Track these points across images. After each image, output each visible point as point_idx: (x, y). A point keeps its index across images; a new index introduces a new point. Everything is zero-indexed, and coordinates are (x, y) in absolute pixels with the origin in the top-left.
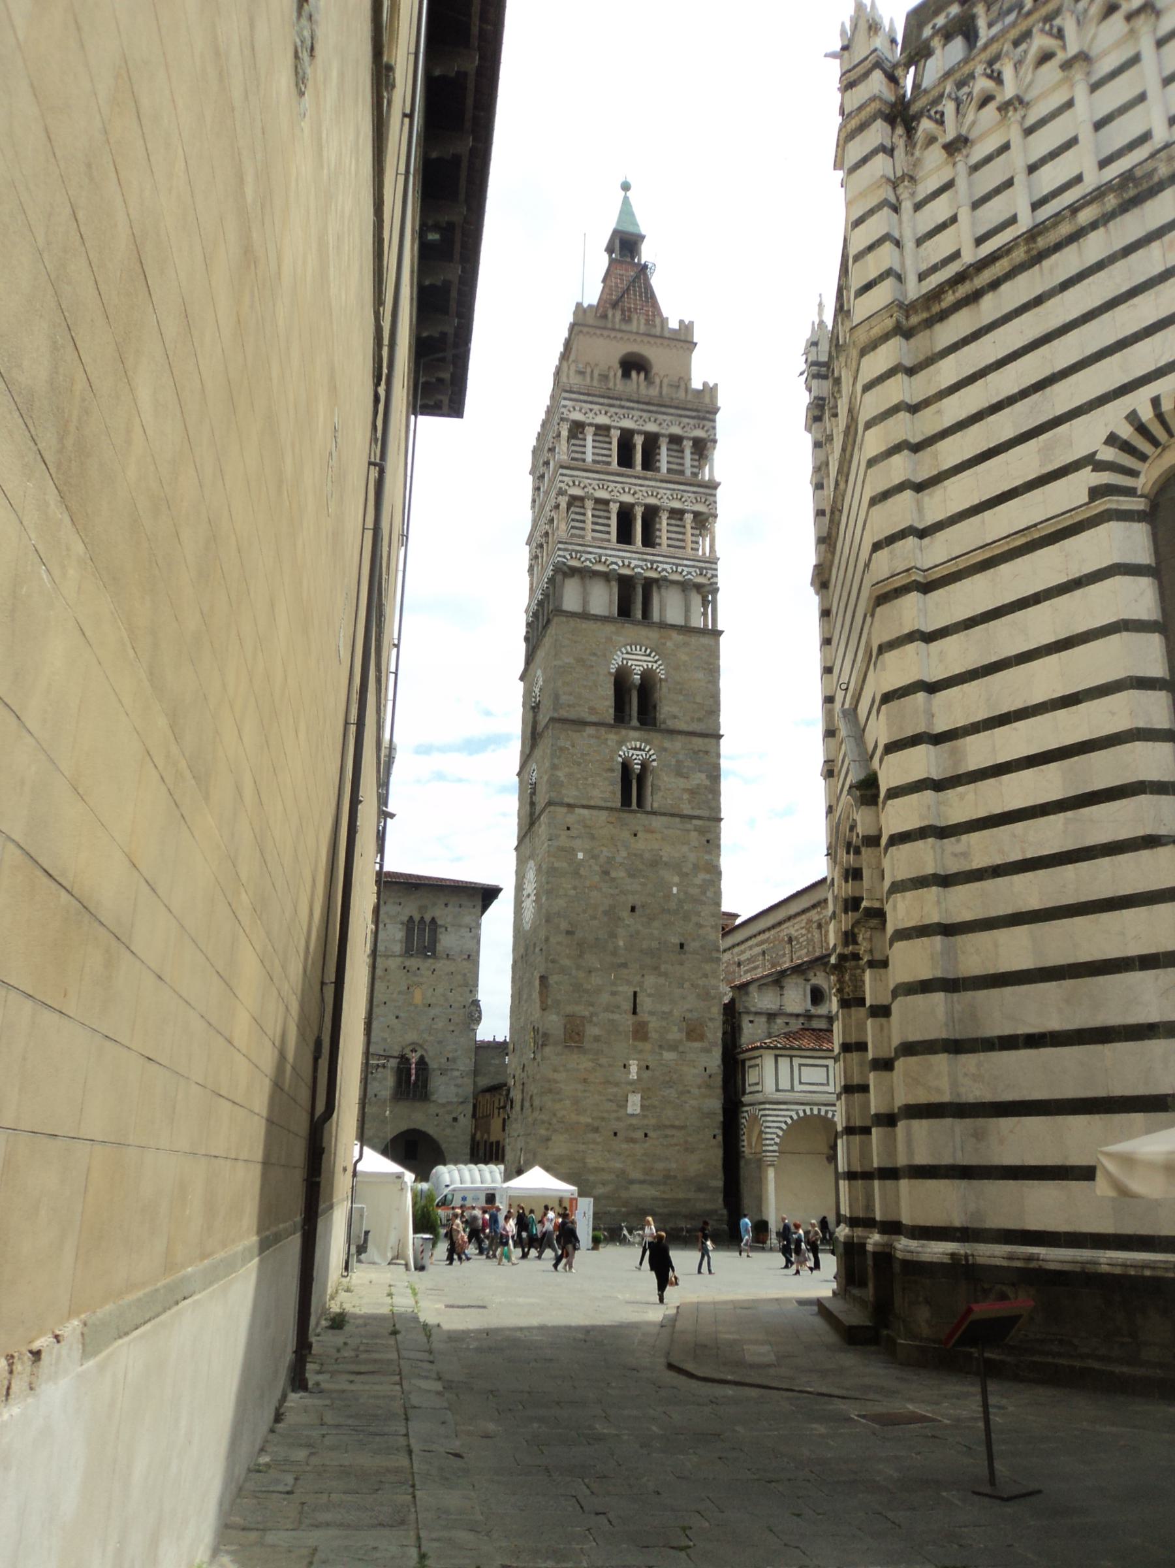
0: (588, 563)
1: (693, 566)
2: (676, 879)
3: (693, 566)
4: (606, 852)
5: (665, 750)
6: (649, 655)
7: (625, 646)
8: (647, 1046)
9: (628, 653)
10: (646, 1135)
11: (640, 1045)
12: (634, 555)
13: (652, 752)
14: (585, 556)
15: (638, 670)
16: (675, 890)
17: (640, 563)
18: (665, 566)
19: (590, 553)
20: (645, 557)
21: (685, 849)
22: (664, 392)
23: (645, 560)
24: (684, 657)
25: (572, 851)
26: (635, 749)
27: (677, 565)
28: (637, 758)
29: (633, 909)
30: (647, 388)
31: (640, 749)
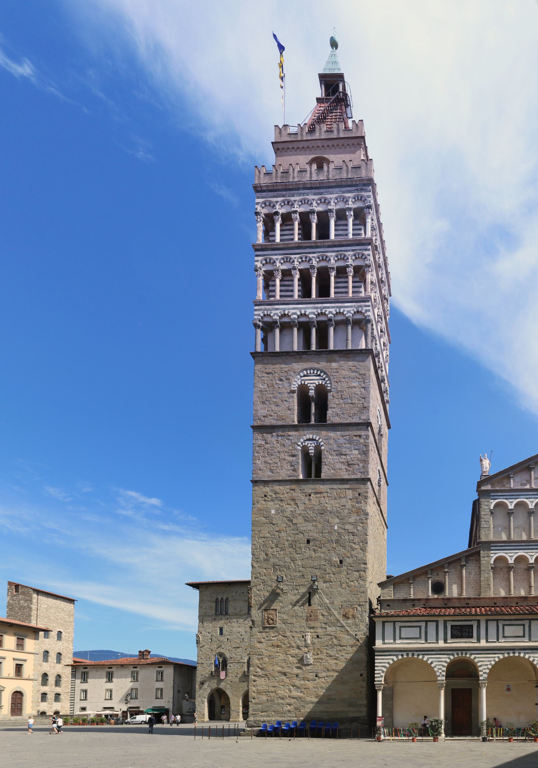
0: (276, 317)
1: (351, 307)
2: (337, 520)
3: (351, 307)
4: (289, 509)
5: (330, 438)
6: (319, 375)
7: (302, 371)
8: (317, 624)
9: (305, 376)
10: (316, 676)
11: (312, 624)
12: (308, 306)
13: (321, 440)
14: (274, 312)
15: (312, 387)
16: (336, 528)
17: (315, 311)
18: (331, 310)
19: (277, 309)
20: (316, 305)
21: (343, 501)
22: (330, 176)
23: (317, 308)
24: (344, 373)
25: (268, 510)
26: (309, 440)
27: (340, 308)
28: (311, 446)
29: (308, 542)
30: (318, 174)
31: (312, 440)
